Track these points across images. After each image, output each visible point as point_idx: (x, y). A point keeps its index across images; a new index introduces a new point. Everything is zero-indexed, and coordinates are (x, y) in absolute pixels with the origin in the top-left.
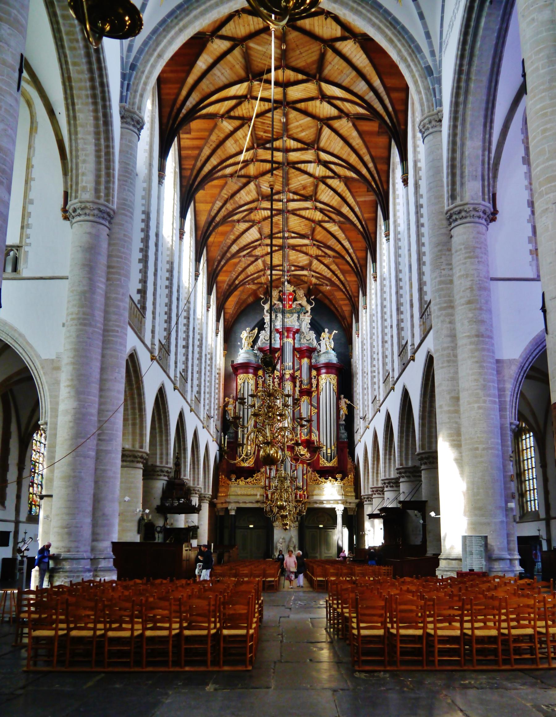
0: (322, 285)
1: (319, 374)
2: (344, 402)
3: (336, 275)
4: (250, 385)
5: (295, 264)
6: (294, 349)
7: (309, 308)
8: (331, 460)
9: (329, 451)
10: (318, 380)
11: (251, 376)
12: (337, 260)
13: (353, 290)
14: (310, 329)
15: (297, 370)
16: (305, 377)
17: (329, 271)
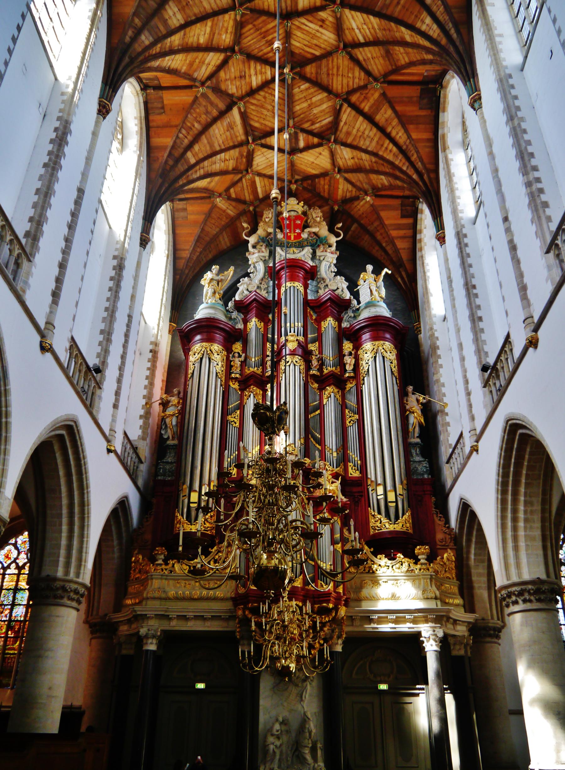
0: (357, 198)
1: (357, 346)
2: (414, 402)
3: (388, 136)
4: (213, 364)
5: (306, 126)
6: (307, 303)
7: (333, 240)
8: (397, 518)
9: (391, 497)
10: (357, 359)
11: (216, 347)
12: (393, 91)
13: (426, 160)
14: (337, 274)
15: (313, 341)
16: (329, 353)
17: (375, 130)
